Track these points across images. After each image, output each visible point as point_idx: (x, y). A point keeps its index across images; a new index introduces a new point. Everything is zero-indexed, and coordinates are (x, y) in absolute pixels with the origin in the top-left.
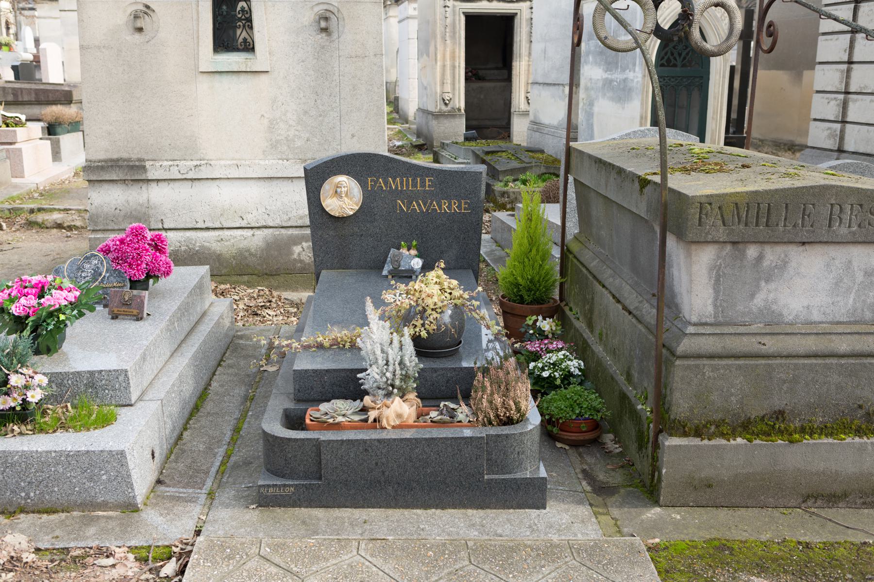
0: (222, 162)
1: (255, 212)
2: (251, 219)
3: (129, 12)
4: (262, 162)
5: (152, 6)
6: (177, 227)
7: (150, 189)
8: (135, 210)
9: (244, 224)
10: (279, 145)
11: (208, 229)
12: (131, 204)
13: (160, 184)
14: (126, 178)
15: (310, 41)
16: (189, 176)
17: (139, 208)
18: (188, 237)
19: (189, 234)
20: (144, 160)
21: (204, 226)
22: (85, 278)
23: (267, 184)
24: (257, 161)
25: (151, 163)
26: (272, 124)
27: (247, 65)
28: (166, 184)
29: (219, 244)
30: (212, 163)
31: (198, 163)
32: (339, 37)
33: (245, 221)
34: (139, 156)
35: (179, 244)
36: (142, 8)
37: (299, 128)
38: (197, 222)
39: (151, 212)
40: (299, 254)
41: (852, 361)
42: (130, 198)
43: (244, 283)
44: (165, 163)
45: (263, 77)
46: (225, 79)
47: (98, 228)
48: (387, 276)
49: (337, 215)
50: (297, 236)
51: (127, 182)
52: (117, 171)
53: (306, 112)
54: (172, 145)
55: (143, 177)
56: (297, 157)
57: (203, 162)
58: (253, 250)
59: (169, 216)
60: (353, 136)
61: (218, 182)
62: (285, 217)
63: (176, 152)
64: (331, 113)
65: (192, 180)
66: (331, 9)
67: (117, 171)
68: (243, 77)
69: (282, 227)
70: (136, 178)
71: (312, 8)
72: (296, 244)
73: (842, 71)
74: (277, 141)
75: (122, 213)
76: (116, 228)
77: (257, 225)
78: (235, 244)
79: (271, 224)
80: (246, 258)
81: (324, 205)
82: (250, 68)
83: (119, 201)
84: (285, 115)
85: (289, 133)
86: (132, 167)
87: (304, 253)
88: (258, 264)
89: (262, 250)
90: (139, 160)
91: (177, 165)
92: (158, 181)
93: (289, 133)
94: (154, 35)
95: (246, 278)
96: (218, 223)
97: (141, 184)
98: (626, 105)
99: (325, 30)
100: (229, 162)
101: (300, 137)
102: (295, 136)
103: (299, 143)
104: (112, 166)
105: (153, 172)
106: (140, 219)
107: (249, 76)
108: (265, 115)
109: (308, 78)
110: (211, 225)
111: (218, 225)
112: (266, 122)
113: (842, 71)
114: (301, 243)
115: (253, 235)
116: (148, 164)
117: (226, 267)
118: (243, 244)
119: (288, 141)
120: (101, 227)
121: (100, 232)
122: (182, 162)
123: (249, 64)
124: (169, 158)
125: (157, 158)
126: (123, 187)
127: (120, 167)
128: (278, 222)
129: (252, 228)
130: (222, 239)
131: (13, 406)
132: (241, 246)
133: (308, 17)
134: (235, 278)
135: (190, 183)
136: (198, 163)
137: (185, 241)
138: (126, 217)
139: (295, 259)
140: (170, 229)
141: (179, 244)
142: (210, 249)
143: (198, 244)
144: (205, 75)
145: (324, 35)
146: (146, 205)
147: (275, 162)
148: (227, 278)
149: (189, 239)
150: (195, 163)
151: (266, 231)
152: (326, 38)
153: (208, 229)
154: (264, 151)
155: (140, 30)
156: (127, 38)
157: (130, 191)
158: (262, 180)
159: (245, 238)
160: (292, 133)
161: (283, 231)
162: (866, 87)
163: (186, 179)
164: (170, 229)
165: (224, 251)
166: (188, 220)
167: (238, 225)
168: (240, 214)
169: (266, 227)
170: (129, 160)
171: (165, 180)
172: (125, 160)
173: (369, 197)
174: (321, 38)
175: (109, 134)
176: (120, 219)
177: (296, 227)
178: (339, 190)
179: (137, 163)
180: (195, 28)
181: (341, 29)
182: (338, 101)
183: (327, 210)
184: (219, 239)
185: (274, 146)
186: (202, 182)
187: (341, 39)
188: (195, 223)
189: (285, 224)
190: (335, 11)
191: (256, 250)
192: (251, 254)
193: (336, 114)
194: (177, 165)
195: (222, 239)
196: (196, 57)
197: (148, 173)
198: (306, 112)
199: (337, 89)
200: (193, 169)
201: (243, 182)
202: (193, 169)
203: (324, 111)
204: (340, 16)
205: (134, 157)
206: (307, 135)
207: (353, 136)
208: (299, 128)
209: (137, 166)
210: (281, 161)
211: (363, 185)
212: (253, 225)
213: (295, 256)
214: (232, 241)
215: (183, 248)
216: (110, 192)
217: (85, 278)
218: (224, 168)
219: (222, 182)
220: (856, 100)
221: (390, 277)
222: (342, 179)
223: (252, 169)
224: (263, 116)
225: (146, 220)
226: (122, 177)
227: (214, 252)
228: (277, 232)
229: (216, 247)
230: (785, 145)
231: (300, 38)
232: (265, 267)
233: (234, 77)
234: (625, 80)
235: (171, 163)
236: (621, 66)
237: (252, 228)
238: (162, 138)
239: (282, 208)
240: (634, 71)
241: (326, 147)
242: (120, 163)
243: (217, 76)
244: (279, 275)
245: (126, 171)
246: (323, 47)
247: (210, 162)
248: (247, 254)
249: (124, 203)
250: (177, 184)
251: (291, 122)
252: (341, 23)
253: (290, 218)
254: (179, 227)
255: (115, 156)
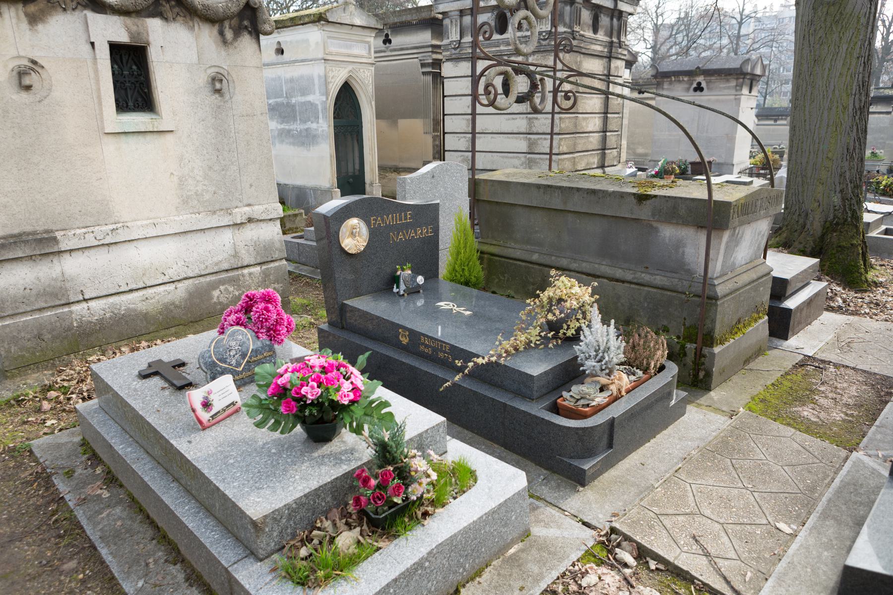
0: (139, 223)
1: (175, 267)
2: (172, 274)
3: (11, 66)
4: (176, 218)
5: (40, 61)
6: (99, 295)
7: (63, 261)
8: (49, 285)
9: (166, 279)
10: (189, 201)
11: (131, 291)
12: (42, 281)
13: (73, 254)
14: (35, 253)
15: (207, 102)
16: (106, 241)
17: (53, 283)
18: (112, 303)
19: (111, 300)
20: (52, 231)
21: (127, 289)
22: (234, 356)
23: (182, 238)
24: (172, 218)
25: (62, 233)
26: (181, 181)
27: (153, 125)
28: (80, 253)
29: (144, 303)
30: (129, 224)
31: (115, 227)
32: (231, 98)
33: (167, 276)
34: (46, 228)
35: (104, 312)
36: (26, 63)
37: (206, 182)
38: (120, 286)
39: (68, 285)
40: (218, 297)
41: (655, 290)
42: (41, 275)
43: (172, 335)
44: (78, 231)
45: (169, 137)
46: (132, 139)
47: (5, 314)
48: (403, 295)
49: (354, 252)
50: (215, 281)
51: (33, 258)
52: (23, 248)
53: (210, 168)
54: (83, 211)
55: (56, 249)
56: (206, 210)
57: (119, 225)
58: (177, 303)
59: (88, 285)
60: (251, 186)
61: (135, 243)
62: (203, 266)
63: (89, 218)
64: (232, 167)
65: (108, 245)
66: (222, 71)
67: (23, 248)
68: (149, 137)
69: (201, 276)
70: (47, 251)
71: (205, 70)
72: (215, 288)
73: (468, 120)
74: (188, 197)
75: (34, 292)
76: (29, 309)
77: (179, 278)
78: (160, 300)
79: (191, 275)
80: (172, 311)
81: (343, 245)
82: (157, 127)
83: (27, 280)
84: (192, 171)
85: (198, 188)
86: (40, 241)
87: (222, 296)
88: (183, 314)
89: (186, 301)
90: (47, 231)
91: (93, 232)
92: (71, 251)
93: (198, 188)
94: (45, 94)
95: (173, 330)
96: (142, 283)
97: (51, 257)
98: (311, 148)
99: (218, 91)
100: (145, 222)
101: (208, 191)
102: (203, 190)
103: (207, 197)
104: (15, 242)
105: (66, 242)
106: (57, 295)
107: (155, 136)
108: (174, 173)
109: (209, 136)
110: (134, 286)
111: (141, 285)
112: (175, 179)
113: (468, 120)
114: (218, 287)
115: (176, 288)
116: (58, 235)
117: (153, 324)
118: (168, 299)
119: (197, 195)
120: (10, 312)
121: (8, 318)
122: (97, 228)
123: (156, 123)
124: (81, 225)
125: (67, 227)
126: (30, 263)
127: (26, 242)
128: (197, 272)
129: (173, 282)
130: (147, 298)
131: (854, 453)
132: (166, 301)
133: (202, 79)
134: (163, 333)
135: (106, 248)
136: (114, 226)
137: (109, 308)
138: (38, 295)
139: (215, 303)
140: (90, 299)
141: (104, 312)
142: (136, 310)
143: (123, 308)
144: (110, 137)
145: (217, 96)
146: (61, 278)
147: (189, 216)
148: (157, 334)
149: (113, 305)
150: (111, 227)
151: (187, 282)
152: (220, 98)
153: (131, 291)
154: (177, 208)
155: (28, 88)
156: (14, 97)
157: (39, 267)
158: (178, 235)
159: (169, 293)
160: (200, 188)
161: (202, 279)
162: (486, 129)
163: (103, 245)
164: (90, 299)
165: (150, 308)
166: (110, 285)
167: (161, 282)
168: (161, 271)
169: (186, 279)
170: (34, 233)
171: (78, 249)
172: (29, 234)
173: (374, 234)
174: (216, 98)
175: (5, 207)
176: (33, 299)
177: (212, 273)
178: (354, 231)
179: (45, 236)
180: (94, 87)
181: (231, 90)
182: (236, 155)
183: (346, 249)
184: (144, 298)
185: (186, 201)
186: (119, 245)
187: (233, 99)
188: (118, 287)
189: (203, 273)
190: (225, 74)
191: (180, 302)
192: (176, 307)
193: (236, 168)
194: (93, 232)
195: (147, 298)
196: (100, 117)
197: (61, 244)
198: (210, 168)
199: (234, 145)
200: (110, 233)
201: (159, 239)
202: (110, 233)
203: (225, 166)
204: (230, 78)
205: (40, 228)
206: (214, 189)
207: (251, 186)
208: (206, 182)
209: (47, 239)
210: (193, 216)
211: (368, 224)
212: (175, 279)
213: (215, 300)
214: (157, 298)
215: (108, 315)
216: (14, 272)
217: (234, 356)
218: (141, 228)
219: (139, 242)
220: (480, 138)
221: (406, 295)
222: (354, 221)
223: (168, 226)
224: (172, 174)
225: (63, 295)
226: (28, 252)
227: (141, 312)
228: (196, 281)
229: (142, 307)
230: (390, 168)
231: (199, 99)
232: (189, 315)
233: (141, 138)
234: (307, 130)
235: (84, 230)
236: (300, 119)
237: (173, 282)
238: (71, 205)
239: (199, 258)
240: (318, 123)
241: (230, 198)
242: (24, 238)
243: (123, 137)
244: (202, 320)
245: (33, 246)
246: (219, 107)
247: (126, 224)
248: (172, 307)
249: (34, 281)
250: (92, 251)
251: (198, 178)
252: (231, 85)
253: (207, 267)
254: (101, 294)
255: (16, 231)
